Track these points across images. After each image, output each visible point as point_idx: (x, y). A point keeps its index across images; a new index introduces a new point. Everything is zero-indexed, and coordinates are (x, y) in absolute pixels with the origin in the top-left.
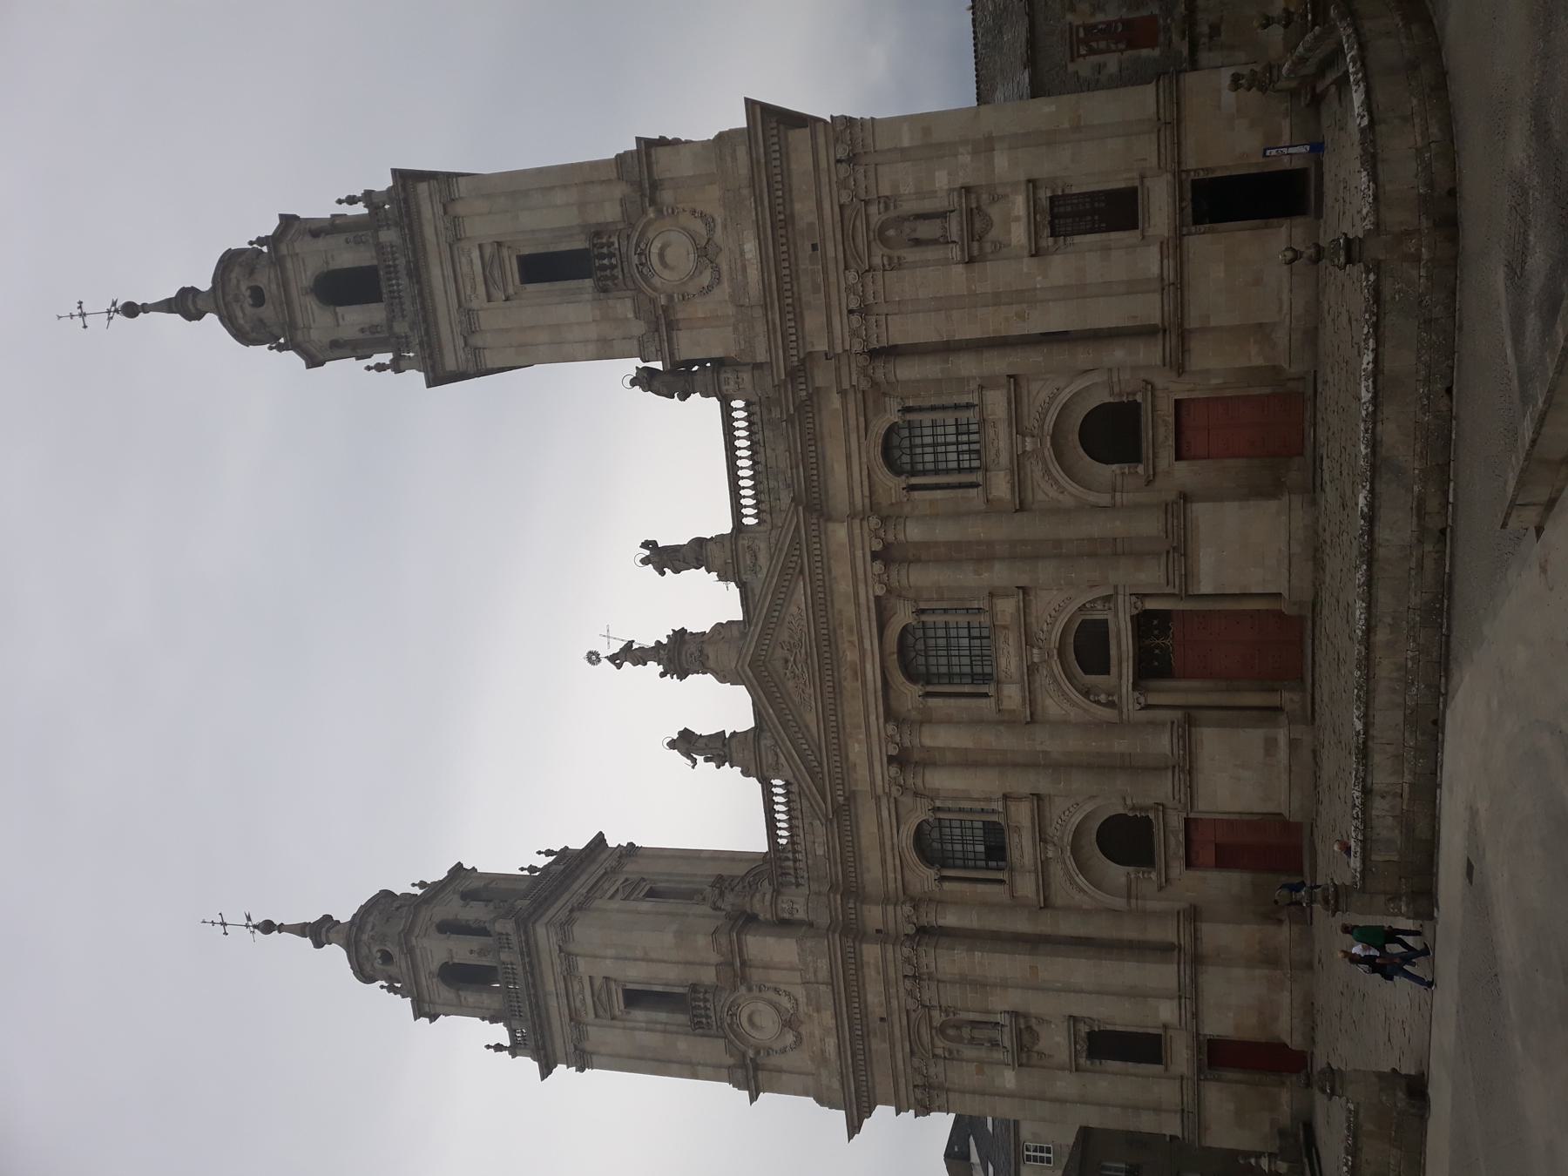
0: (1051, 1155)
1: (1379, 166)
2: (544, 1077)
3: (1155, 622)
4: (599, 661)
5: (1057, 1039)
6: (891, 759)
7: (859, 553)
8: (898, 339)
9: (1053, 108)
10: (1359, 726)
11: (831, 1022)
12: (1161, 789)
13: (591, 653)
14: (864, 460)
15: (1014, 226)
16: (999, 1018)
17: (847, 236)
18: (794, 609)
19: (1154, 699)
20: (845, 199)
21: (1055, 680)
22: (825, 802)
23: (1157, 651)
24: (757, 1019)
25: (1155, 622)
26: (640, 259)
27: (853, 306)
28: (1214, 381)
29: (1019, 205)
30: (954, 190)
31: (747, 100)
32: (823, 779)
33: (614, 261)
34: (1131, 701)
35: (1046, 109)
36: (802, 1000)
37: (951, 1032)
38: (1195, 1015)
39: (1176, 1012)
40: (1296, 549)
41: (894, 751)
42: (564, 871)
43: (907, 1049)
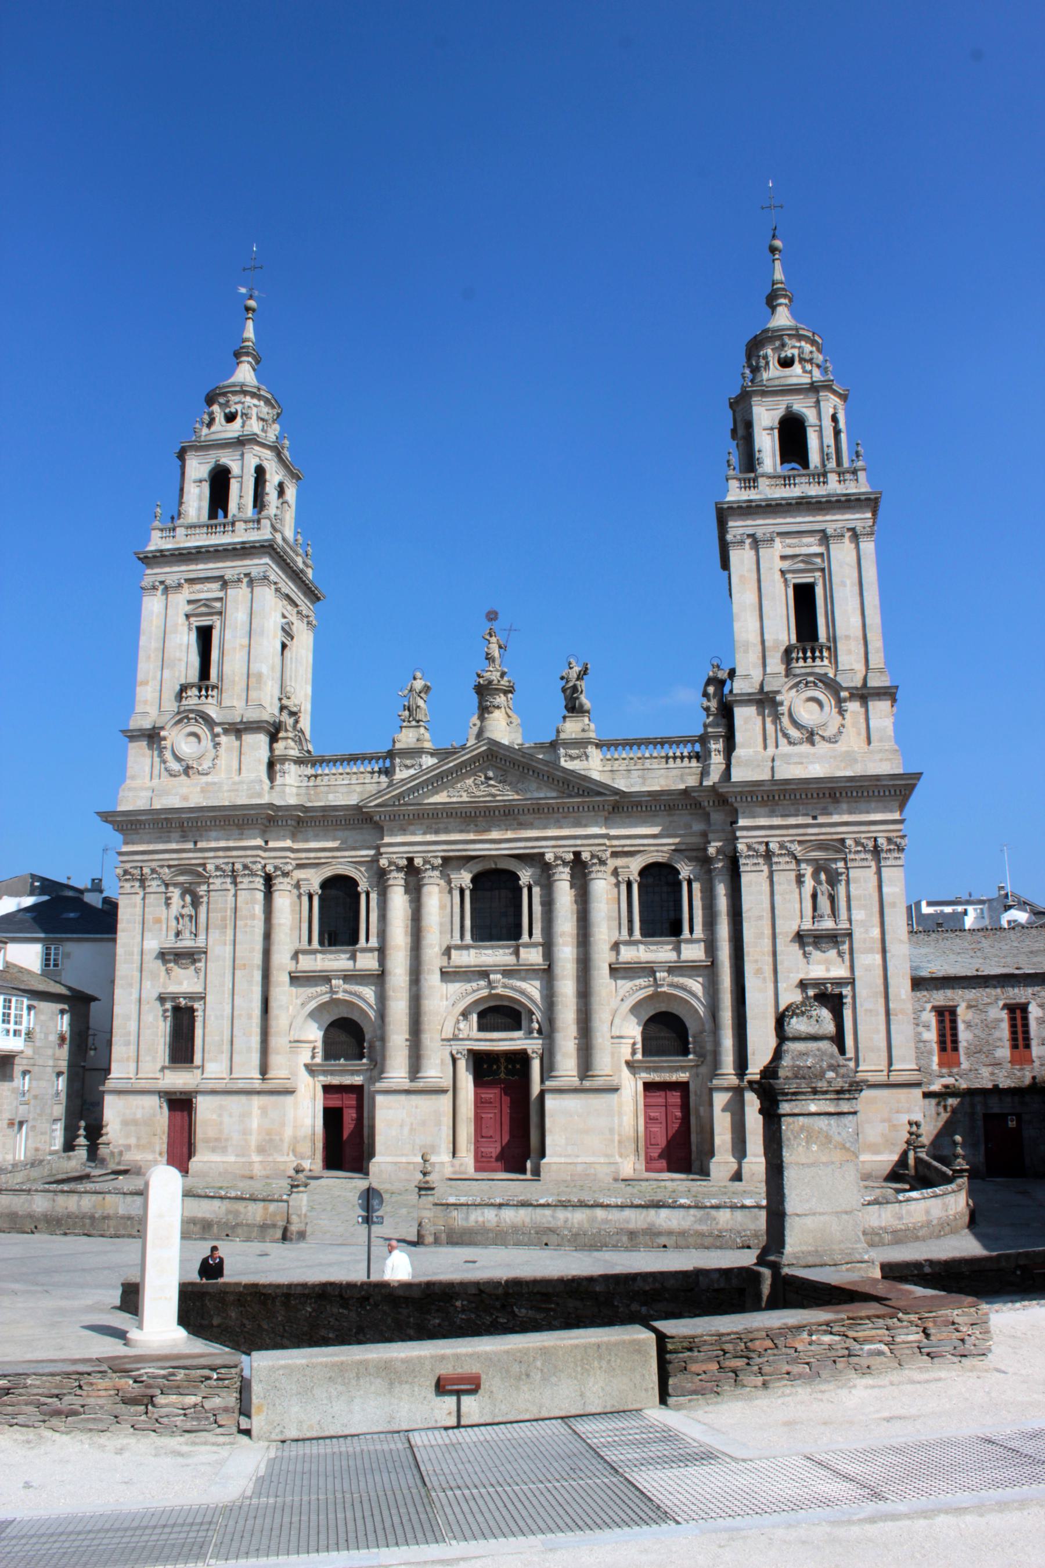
0: (52, 967)
1: (877, 1206)
2: (136, 554)
3: (518, 1066)
4: (490, 620)
5: (185, 983)
6: (410, 860)
7: (579, 842)
8: (745, 879)
9: (903, 997)
10: (542, 1201)
11: (191, 804)
12: (397, 1070)
13: (496, 613)
14: (652, 848)
15: (823, 967)
16: (202, 937)
17: (822, 846)
18: (534, 786)
19: (462, 1064)
20: (849, 842)
21: (474, 991)
22: (376, 806)
23: (495, 1067)
24: (193, 739)
25: (518, 1066)
26: (810, 682)
27: (771, 845)
28: (702, 1109)
29: (840, 971)
30: (851, 924)
31: (921, 774)
32: (394, 805)
33: (809, 660)
34: (459, 1048)
35: (903, 992)
36: (209, 779)
37: (188, 898)
38: (213, 1092)
39: (213, 1076)
40: (579, 1168)
41: (418, 862)
42: (297, 567)
43: (172, 863)
